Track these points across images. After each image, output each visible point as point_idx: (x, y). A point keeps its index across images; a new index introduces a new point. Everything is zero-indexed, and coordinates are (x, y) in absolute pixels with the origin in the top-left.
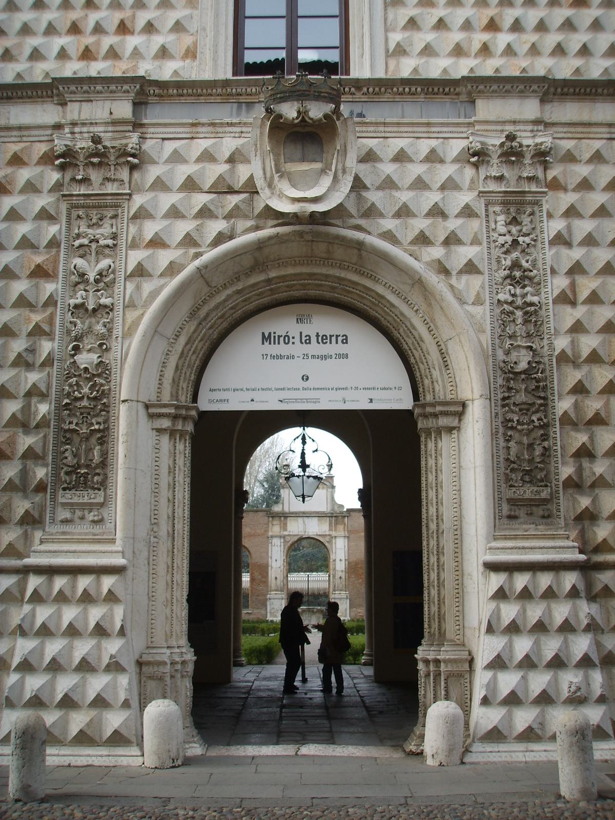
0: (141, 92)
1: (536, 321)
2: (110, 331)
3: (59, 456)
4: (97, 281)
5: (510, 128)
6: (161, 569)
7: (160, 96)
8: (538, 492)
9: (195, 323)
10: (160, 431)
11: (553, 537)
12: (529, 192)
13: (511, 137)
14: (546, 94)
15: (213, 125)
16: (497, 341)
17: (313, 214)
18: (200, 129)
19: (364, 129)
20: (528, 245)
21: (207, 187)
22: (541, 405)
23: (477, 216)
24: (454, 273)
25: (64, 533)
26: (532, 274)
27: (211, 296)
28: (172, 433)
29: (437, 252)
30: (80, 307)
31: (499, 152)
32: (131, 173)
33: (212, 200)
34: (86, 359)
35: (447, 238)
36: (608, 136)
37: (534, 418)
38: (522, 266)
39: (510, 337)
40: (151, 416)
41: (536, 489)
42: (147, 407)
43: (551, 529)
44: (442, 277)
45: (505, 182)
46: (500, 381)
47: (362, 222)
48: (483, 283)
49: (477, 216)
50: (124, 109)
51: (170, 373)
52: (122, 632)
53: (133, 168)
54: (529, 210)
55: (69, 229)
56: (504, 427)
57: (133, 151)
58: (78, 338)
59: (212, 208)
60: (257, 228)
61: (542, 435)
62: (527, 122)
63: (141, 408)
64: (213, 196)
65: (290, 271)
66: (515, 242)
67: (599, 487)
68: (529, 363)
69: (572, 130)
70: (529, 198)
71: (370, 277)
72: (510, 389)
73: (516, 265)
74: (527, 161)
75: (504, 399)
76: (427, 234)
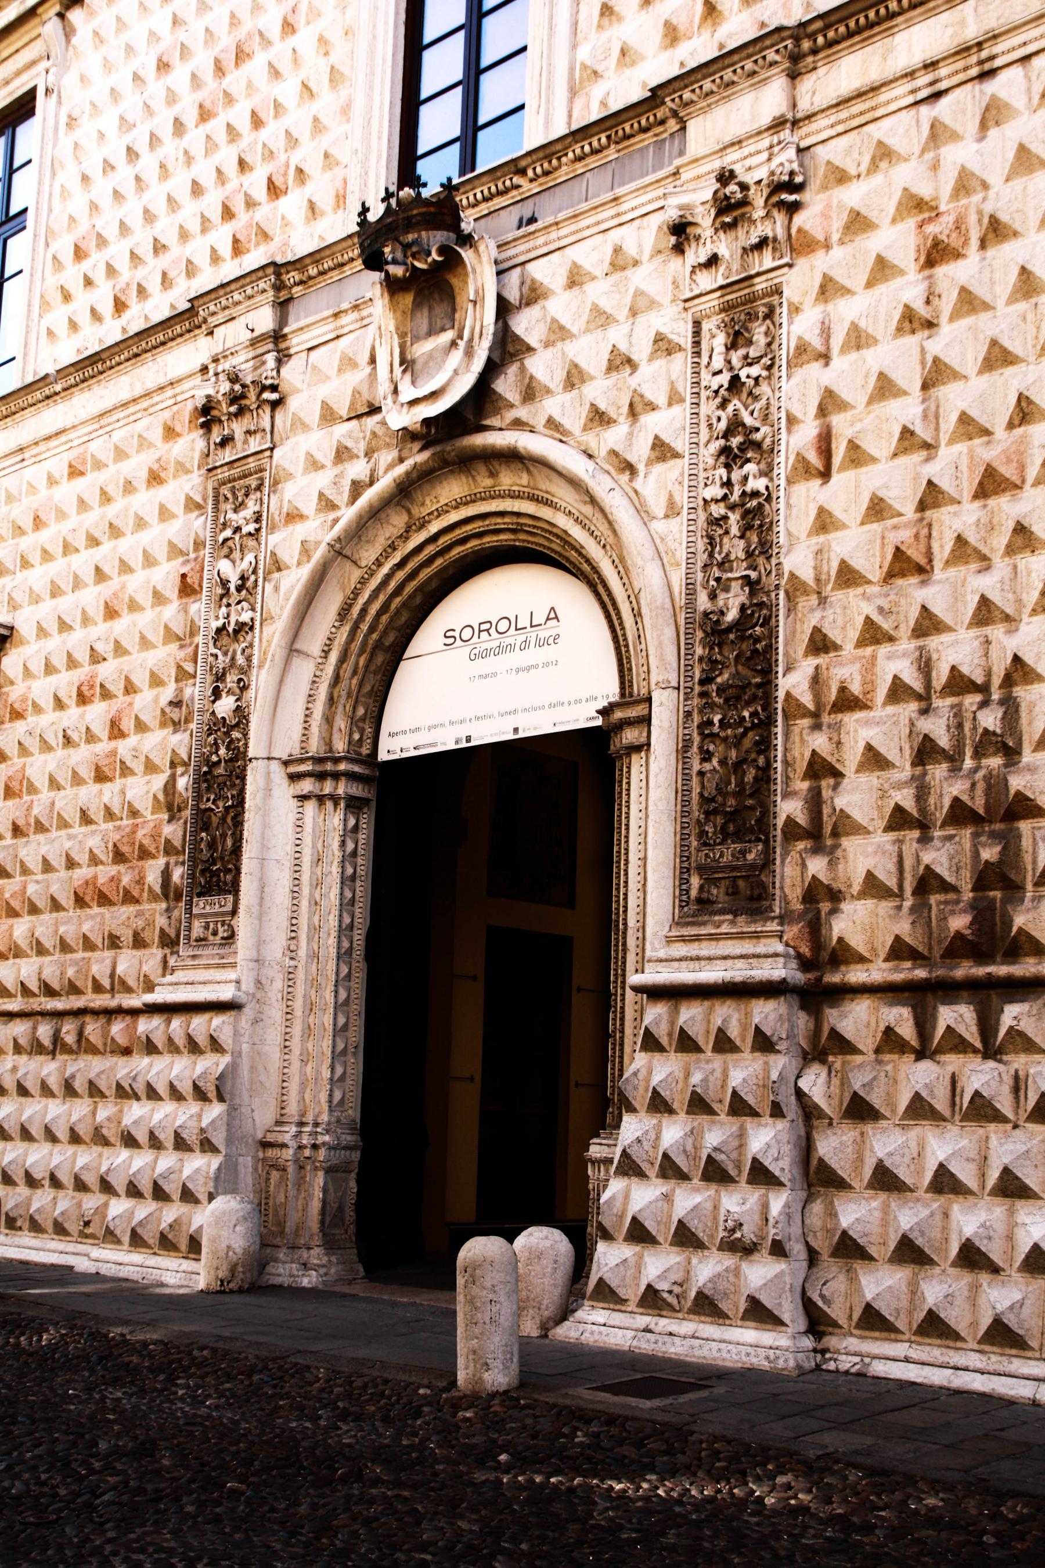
0: (279, 287)
1: (761, 526)
2: (249, 659)
3: (196, 849)
4: (239, 589)
5: (716, 164)
6: (298, 1005)
7: (302, 282)
8: (743, 853)
9: (347, 628)
10: (303, 798)
11: (756, 936)
12: (758, 274)
13: (725, 177)
14: (795, 58)
15: (356, 307)
16: (700, 576)
17: (427, 422)
18: (345, 320)
19: (531, 244)
20: (756, 379)
21: (344, 413)
22: (758, 686)
23: (680, 349)
24: (641, 467)
25: (194, 957)
26: (758, 436)
27: (363, 582)
28: (321, 799)
29: (613, 437)
30: (220, 631)
31: (713, 212)
32: (272, 417)
33: (349, 434)
34: (225, 706)
35: (631, 405)
36: (911, 99)
37: (746, 714)
38: (744, 425)
39: (721, 565)
40: (294, 778)
41: (738, 846)
42: (286, 763)
43: (755, 922)
44: (625, 477)
45: (722, 269)
46: (699, 651)
47: (522, 413)
48: (682, 474)
49: (680, 349)
50: (264, 319)
51: (319, 709)
52: (221, 1098)
53: (275, 405)
54: (762, 310)
55: (216, 519)
56: (700, 737)
57: (269, 382)
58: (220, 677)
59: (349, 444)
60: (401, 460)
61: (756, 743)
62: (759, 133)
63: (275, 766)
64: (354, 422)
65: (454, 517)
66: (735, 383)
67: (848, 834)
68: (743, 608)
69: (844, 115)
70: (760, 285)
71: (548, 503)
72: (713, 663)
73: (735, 425)
74: (759, 213)
75: (702, 682)
76: (602, 407)
